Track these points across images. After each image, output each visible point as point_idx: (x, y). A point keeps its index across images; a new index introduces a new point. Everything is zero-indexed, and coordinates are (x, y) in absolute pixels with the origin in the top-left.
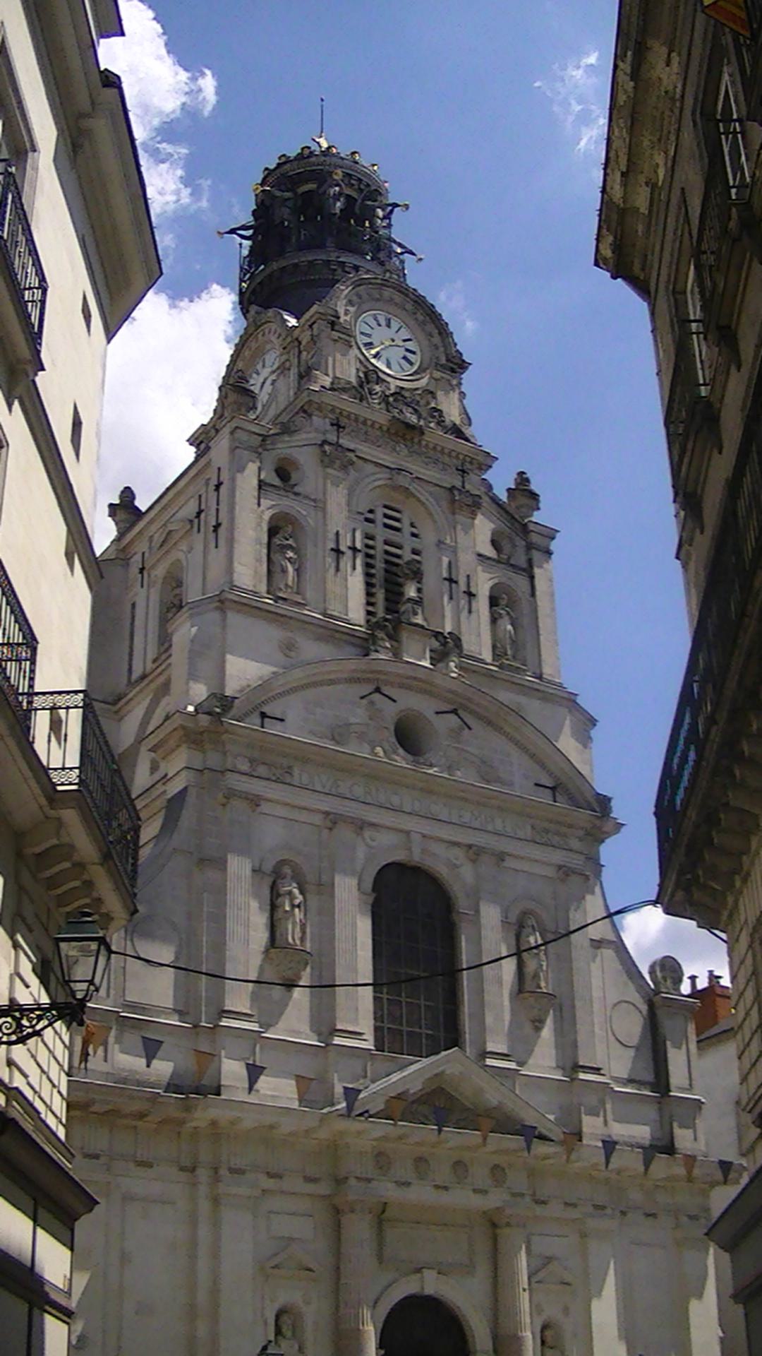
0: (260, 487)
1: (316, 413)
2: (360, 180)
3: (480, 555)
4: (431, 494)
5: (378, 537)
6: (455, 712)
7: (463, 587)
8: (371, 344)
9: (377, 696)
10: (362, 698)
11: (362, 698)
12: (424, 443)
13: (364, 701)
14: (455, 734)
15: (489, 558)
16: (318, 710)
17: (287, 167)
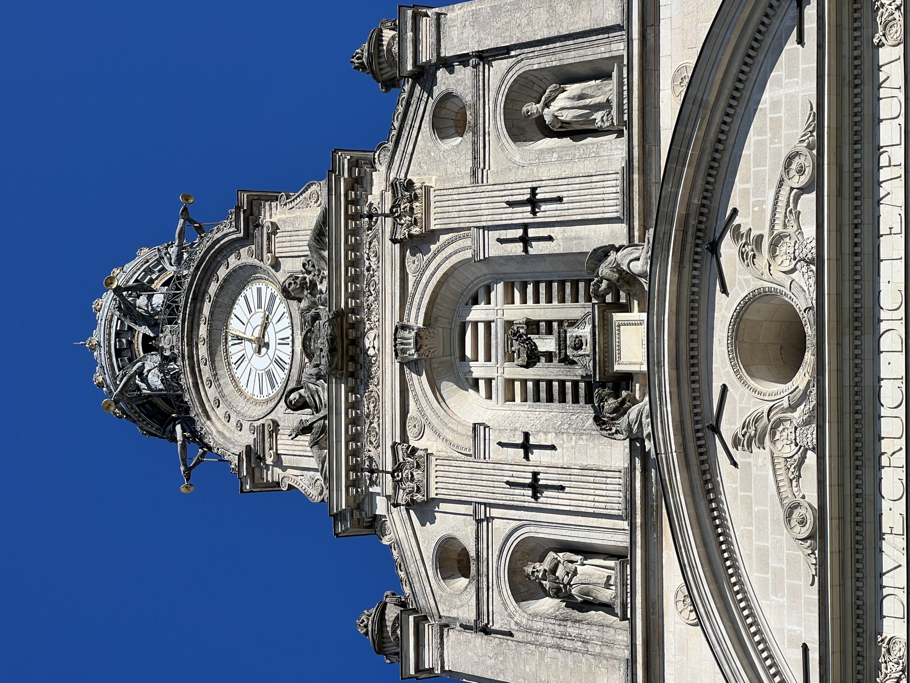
0: (486, 631)
1: (367, 508)
2: (118, 334)
3: (474, 173)
4: (417, 283)
5: (507, 376)
6: (714, 248)
7: (523, 214)
8: (276, 362)
9: (729, 427)
10: (735, 464)
11: (735, 464)
12: (352, 303)
13: (737, 455)
14: (751, 248)
15: (475, 152)
16: (772, 563)
17: (153, 431)
